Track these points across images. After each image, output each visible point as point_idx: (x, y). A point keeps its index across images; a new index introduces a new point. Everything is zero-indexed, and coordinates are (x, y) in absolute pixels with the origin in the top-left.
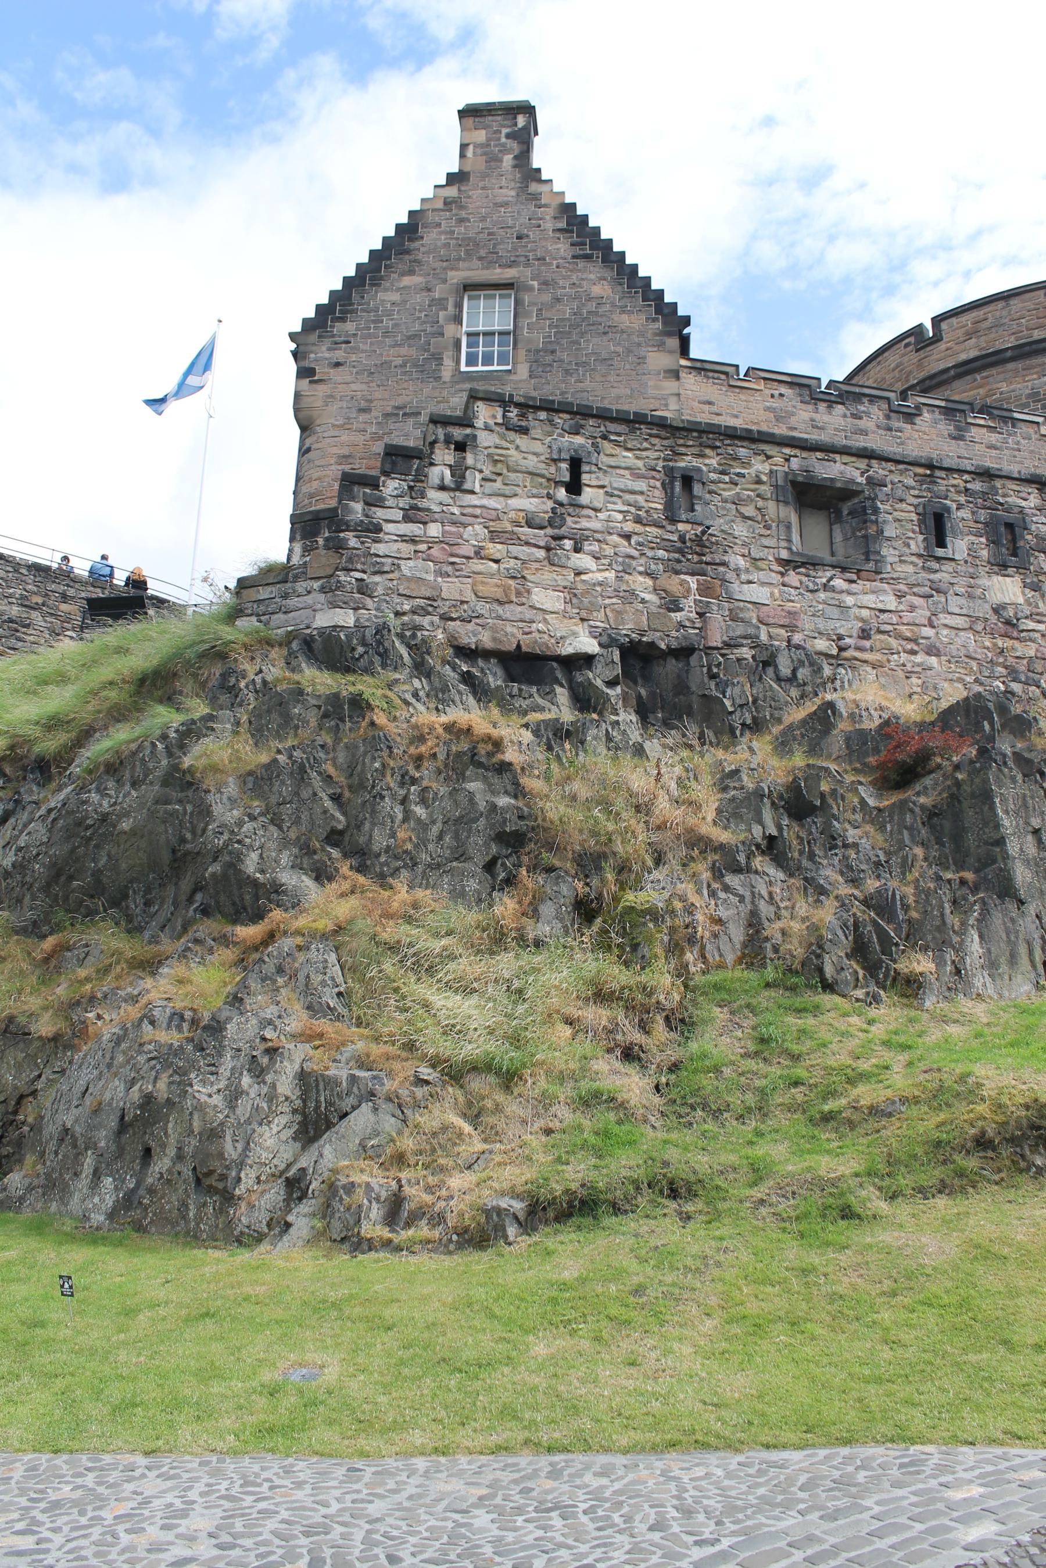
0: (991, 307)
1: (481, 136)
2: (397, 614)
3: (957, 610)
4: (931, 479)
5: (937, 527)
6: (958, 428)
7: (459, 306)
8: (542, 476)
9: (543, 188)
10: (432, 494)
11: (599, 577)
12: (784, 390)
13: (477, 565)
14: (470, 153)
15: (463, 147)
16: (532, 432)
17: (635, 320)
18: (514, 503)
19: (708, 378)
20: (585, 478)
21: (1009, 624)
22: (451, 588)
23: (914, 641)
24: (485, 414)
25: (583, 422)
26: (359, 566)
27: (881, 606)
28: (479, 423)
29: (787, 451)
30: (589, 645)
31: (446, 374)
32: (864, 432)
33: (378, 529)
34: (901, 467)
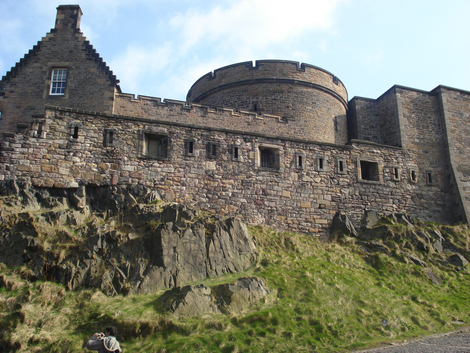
0: (230, 69)
1: (62, 16)
3: (193, 172)
4: (190, 131)
7: (50, 74)
8: (65, 133)
9: (79, 35)
11: (80, 164)
12: (148, 102)
13: (43, 161)
14: (58, 23)
15: (57, 20)
17: (103, 81)
18: (56, 141)
21: (210, 176)
22: (34, 168)
23: (179, 182)
26: (7, 162)
28: (47, 116)
29: (144, 123)
30: (75, 184)
31: (44, 96)
34: (181, 128)
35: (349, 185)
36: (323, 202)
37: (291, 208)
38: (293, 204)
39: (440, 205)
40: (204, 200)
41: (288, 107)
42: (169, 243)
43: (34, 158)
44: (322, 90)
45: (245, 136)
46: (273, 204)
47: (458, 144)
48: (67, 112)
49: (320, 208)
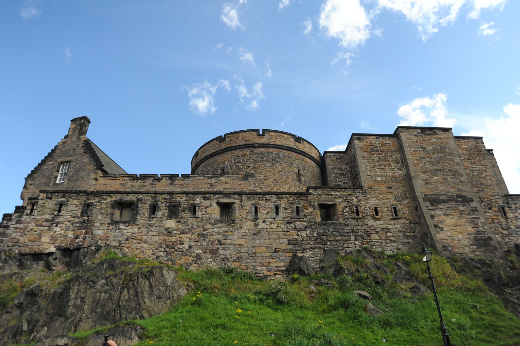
5: (154, 209)
6: (172, 181)
7: (59, 168)
10: (25, 217)
11: (60, 233)
12: (126, 178)
13: (31, 233)
16: (53, 199)
18: (43, 217)
20: (62, 208)
21: (169, 232)
22: (22, 239)
23: (141, 240)
24: (42, 195)
28: (40, 198)
29: (117, 195)
30: (53, 249)
31: (51, 185)
32: (145, 186)
33: (9, 226)
35: (306, 228)
36: (279, 246)
37: (246, 254)
38: (248, 250)
39: (410, 237)
40: (162, 254)
41: (249, 167)
42: (77, 293)
43: (23, 233)
44: (283, 149)
45: (203, 196)
46: (227, 252)
47: (423, 176)
49: (276, 252)
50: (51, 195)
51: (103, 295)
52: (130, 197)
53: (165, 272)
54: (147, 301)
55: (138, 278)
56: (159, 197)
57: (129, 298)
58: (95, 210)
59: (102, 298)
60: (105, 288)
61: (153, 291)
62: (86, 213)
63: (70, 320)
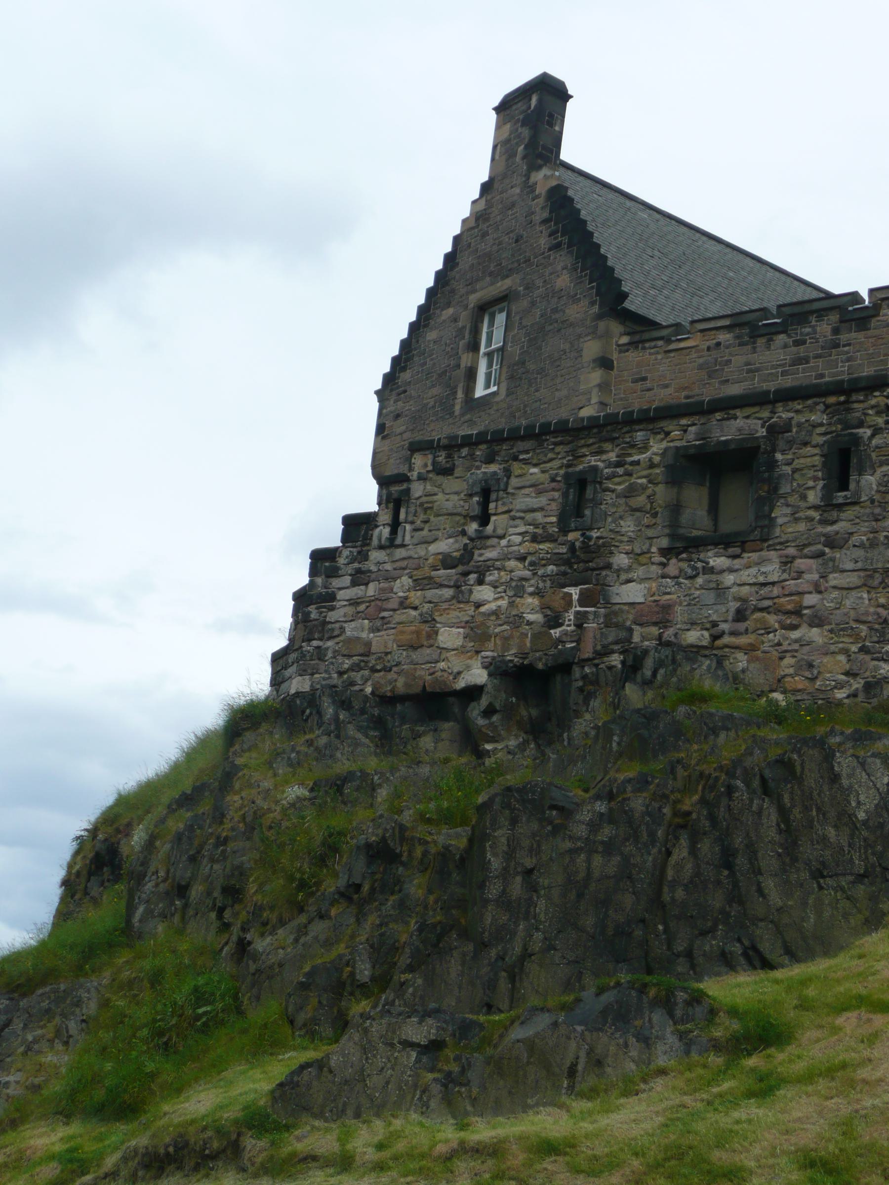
2: (341, 674)
3: (850, 566)
7: (476, 332)
10: (376, 555)
11: (493, 606)
13: (399, 617)
16: (458, 472)
18: (433, 548)
19: (644, 348)
20: (492, 506)
22: (380, 641)
24: (420, 462)
25: (497, 448)
27: (761, 579)
29: (684, 422)
30: (478, 675)
31: (457, 408)
33: (332, 597)
42: (510, 855)
48: (462, 446)
50: (449, 456)
51: (597, 860)
52: (740, 422)
53: (844, 763)
54: (769, 884)
55: (730, 790)
56: (861, 406)
57: (698, 874)
58: (609, 497)
59: (596, 874)
60: (606, 832)
61: (795, 843)
62: (579, 514)
63: (493, 953)
